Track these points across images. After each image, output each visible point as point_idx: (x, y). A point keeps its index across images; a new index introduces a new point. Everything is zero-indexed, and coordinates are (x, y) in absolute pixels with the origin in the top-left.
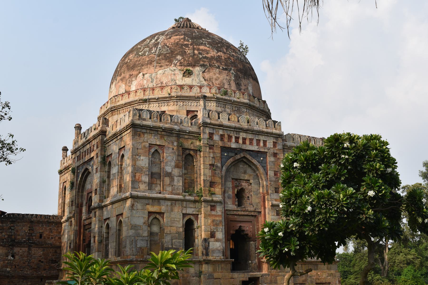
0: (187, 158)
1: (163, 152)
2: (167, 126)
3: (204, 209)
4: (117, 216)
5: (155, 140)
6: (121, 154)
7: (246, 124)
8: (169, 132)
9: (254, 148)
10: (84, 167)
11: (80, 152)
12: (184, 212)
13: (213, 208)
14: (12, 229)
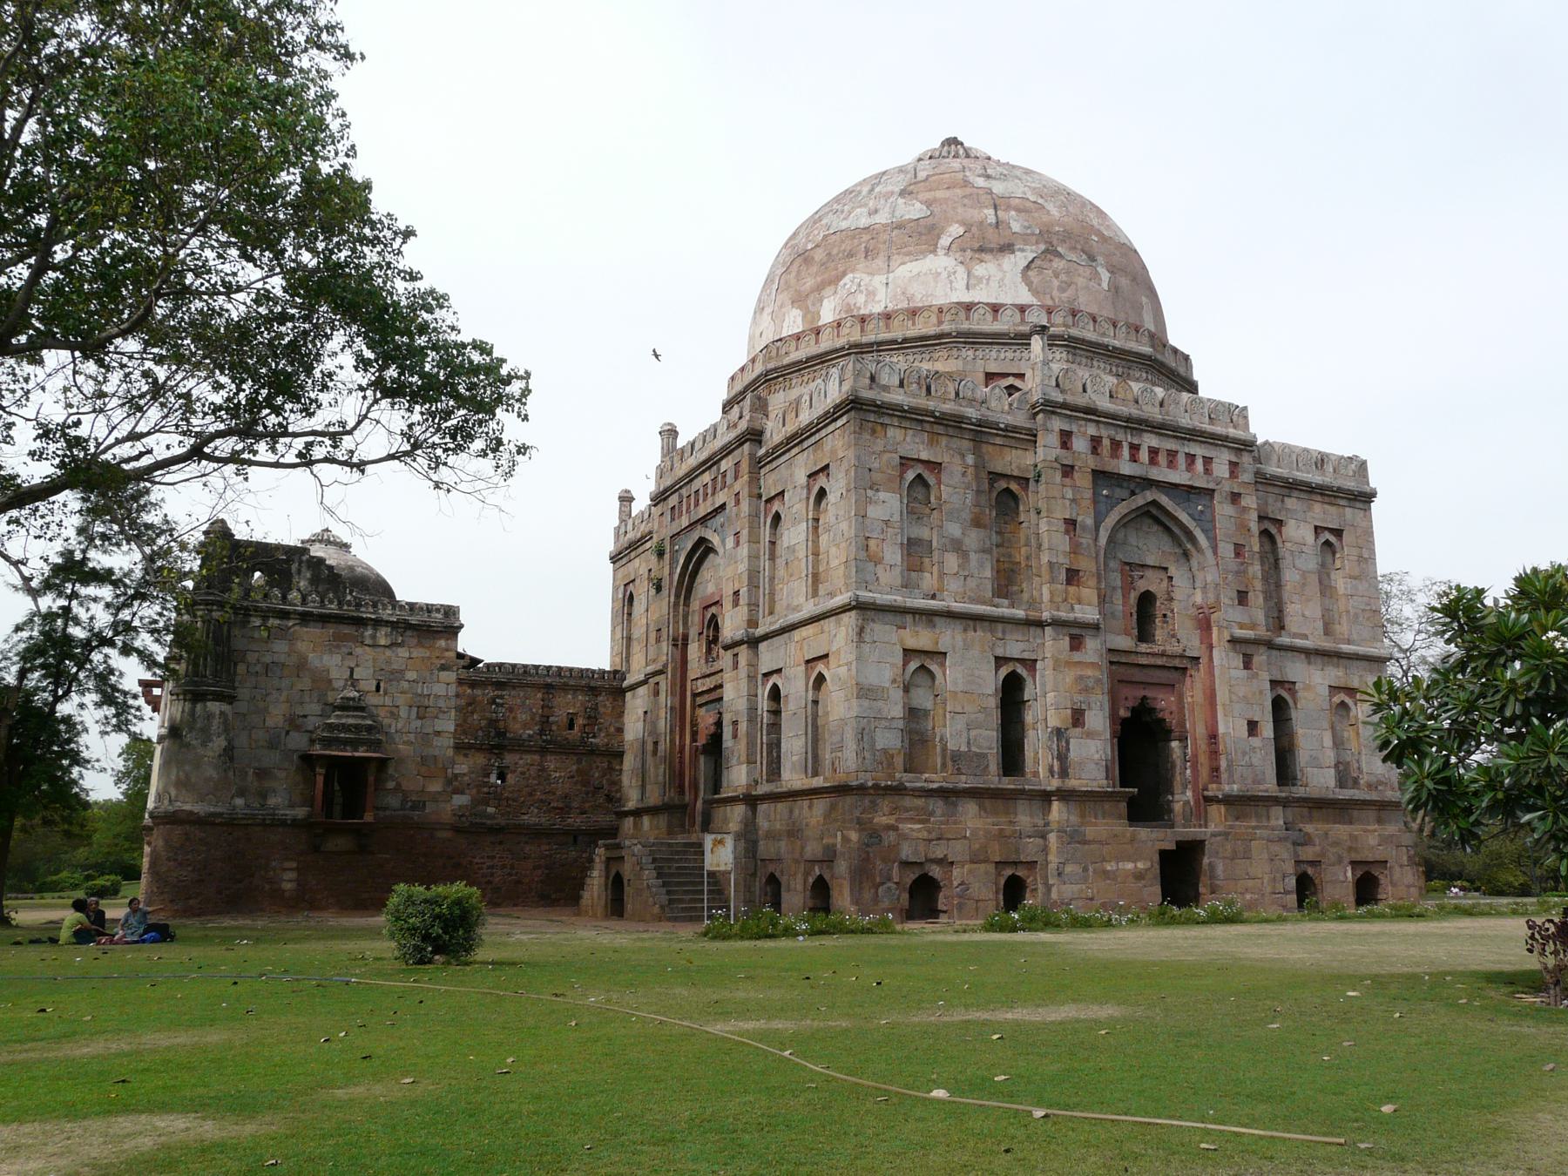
0: (1004, 499)
1: (939, 483)
2: (948, 407)
3: (1052, 645)
4: (808, 662)
6: (815, 490)
7: (1157, 409)
8: (951, 424)
9: (1178, 476)
10: (695, 536)
11: (681, 496)
12: (1000, 652)
13: (1076, 643)
14: (498, 705)
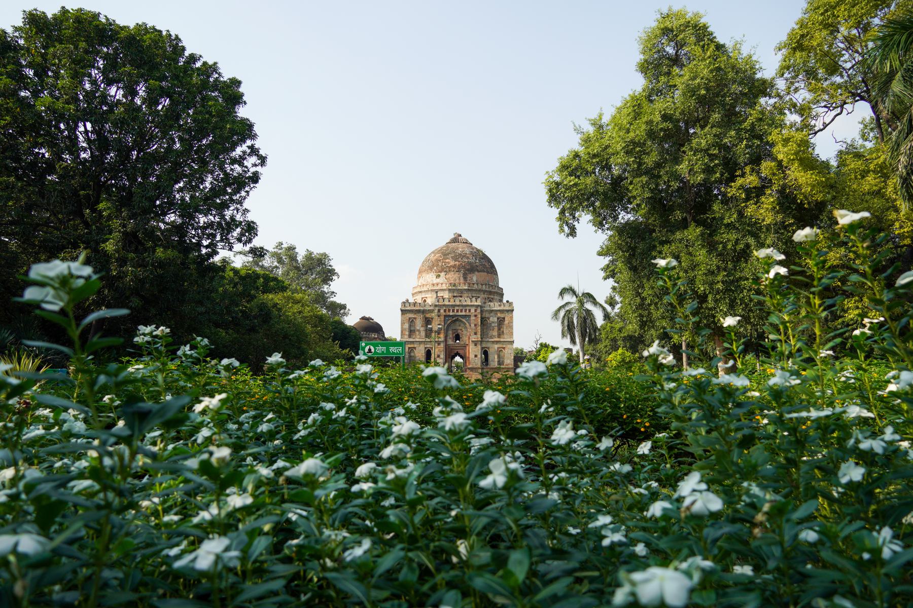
0: (428, 321)
5: (412, 316)
8: (418, 311)
9: (463, 313)
13: (439, 344)
